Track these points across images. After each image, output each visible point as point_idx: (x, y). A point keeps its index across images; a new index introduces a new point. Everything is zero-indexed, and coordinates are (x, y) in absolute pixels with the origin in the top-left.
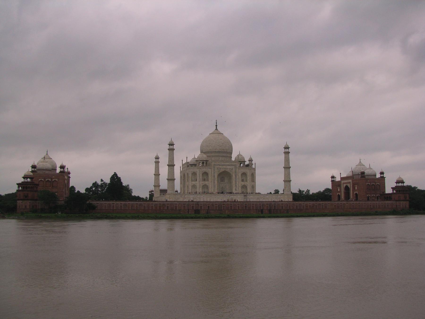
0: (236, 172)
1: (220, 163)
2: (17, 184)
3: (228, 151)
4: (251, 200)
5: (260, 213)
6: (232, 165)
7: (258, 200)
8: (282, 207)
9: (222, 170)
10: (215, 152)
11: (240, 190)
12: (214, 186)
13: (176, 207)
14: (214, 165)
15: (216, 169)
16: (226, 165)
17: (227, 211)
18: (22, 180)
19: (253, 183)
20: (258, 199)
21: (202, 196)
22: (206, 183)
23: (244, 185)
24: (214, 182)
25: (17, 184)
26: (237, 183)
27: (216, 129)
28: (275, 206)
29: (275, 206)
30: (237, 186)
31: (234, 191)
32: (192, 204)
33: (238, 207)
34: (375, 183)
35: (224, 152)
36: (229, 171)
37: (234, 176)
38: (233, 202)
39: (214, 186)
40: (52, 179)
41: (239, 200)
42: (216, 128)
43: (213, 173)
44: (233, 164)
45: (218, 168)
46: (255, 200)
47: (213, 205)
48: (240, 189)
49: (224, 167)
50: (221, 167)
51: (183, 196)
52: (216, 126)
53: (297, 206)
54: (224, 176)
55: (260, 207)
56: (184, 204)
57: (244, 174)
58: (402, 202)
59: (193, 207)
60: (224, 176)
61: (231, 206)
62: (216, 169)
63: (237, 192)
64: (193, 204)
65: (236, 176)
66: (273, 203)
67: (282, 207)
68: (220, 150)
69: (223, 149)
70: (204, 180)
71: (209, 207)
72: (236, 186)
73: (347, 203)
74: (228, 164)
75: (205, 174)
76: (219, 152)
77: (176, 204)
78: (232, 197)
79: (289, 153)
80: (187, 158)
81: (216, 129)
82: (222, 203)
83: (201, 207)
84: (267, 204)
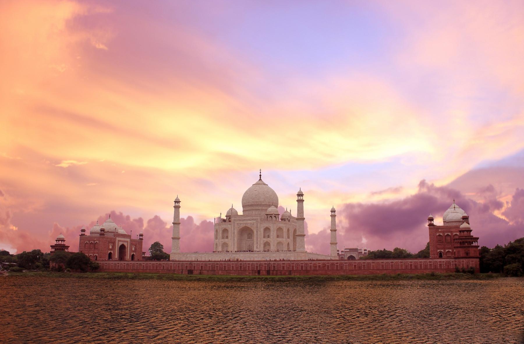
0: (257, 227)
1: (240, 218)
2: (51, 246)
5: (257, 274)
6: (253, 219)
7: (264, 259)
8: (283, 267)
9: (243, 226)
12: (234, 244)
13: (171, 266)
14: (235, 220)
15: (236, 224)
17: (220, 272)
18: (54, 243)
19: (280, 239)
20: (263, 258)
25: (51, 246)
26: (259, 239)
27: (260, 179)
28: (274, 267)
29: (274, 267)
31: (255, 249)
33: (233, 266)
34: (452, 232)
35: (257, 205)
37: (255, 232)
38: (235, 261)
39: (234, 244)
40: (94, 241)
46: (260, 259)
47: (206, 265)
48: (262, 246)
49: (245, 222)
50: (241, 222)
52: (260, 176)
53: (302, 267)
55: (257, 267)
57: (267, 229)
58: (461, 260)
59: (187, 266)
60: (246, 232)
61: (225, 267)
62: (236, 224)
63: (258, 250)
65: (257, 232)
67: (283, 267)
72: (257, 243)
73: (373, 263)
74: (249, 218)
75: (225, 231)
76: (252, 205)
78: (235, 255)
79: (302, 201)
81: (260, 179)
82: (216, 263)
83: (194, 266)
84: (265, 264)
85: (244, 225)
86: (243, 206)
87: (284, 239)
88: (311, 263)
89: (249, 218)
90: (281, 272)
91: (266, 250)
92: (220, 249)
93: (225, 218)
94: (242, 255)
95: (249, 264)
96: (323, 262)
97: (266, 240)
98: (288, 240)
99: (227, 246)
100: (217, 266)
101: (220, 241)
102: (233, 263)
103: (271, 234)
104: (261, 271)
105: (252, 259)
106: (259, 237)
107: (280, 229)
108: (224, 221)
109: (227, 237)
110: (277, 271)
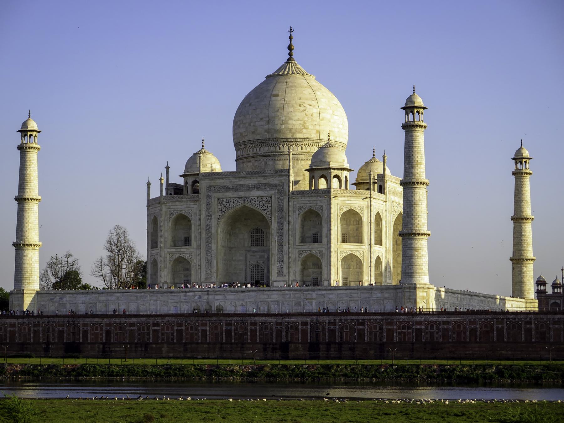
0: (280, 210)
3: (298, 135)
4: (274, 309)
6: (266, 186)
7: (299, 310)
10: (254, 141)
11: (294, 273)
12: (209, 262)
13: (13, 334)
14: (210, 188)
15: (214, 202)
16: (250, 188)
17: (165, 349)
21: (113, 298)
22: (184, 251)
23: (311, 256)
24: (209, 249)
26: (285, 248)
27: (290, 60)
28: (332, 332)
30: (285, 259)
31: (274, 276)
32: (59, 325)
33: (204, 331)
36: (258, 209)
37: (274, 226)
41: (229, 309)
42: (290, 54)
43: (203, 216)
44: (271, 180)
45: (219, 199)
46: (285, 308)
48: (296, 268)
49: (241, 194)
50: (229, 194)
51: (57, 299)
52: (290, 48)
54: (251, 226)
55: (279, 332)
56: (35, 325)
61: (180, 332)
62: (214, 202)
64: (63, 325)
66: (326, 318)
67: (361, 334)
68: (268, 136)
69: (279, 131)
70: (187, 242)
71: (108, 333)
72: (281, 259)
74: (254, 181)
75: (182, 221)
77: (13, 325)
80: (167, 168)
82: (151, 320)
83: (85, 332)
84: (306, 324)
85: (240, 204)
86: (237, 145)
87: (364, 247)
88: (445, 323)
89: (254, 181)
90: (352, 350)
91: (310, 279)
92: (165, 276)
93: (181, 181)
94: (231, 296)
95: (255, 324)
96: (483, 317)
97: (307, 248)
98: (375, 248)
99: (188, 270)
100: (156, 331)
101: (167, 253)
102: (206, 320)
103: (324, 231)
104: (292, 347)
105: (264, 309)
106: (285, 240)
107: (352, 218)
108: (176, 190)
109: (187, 242)
110: (340, 344)
